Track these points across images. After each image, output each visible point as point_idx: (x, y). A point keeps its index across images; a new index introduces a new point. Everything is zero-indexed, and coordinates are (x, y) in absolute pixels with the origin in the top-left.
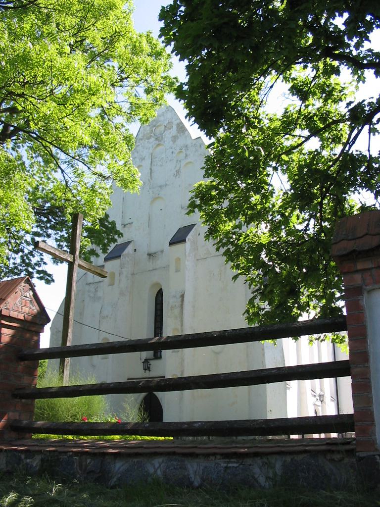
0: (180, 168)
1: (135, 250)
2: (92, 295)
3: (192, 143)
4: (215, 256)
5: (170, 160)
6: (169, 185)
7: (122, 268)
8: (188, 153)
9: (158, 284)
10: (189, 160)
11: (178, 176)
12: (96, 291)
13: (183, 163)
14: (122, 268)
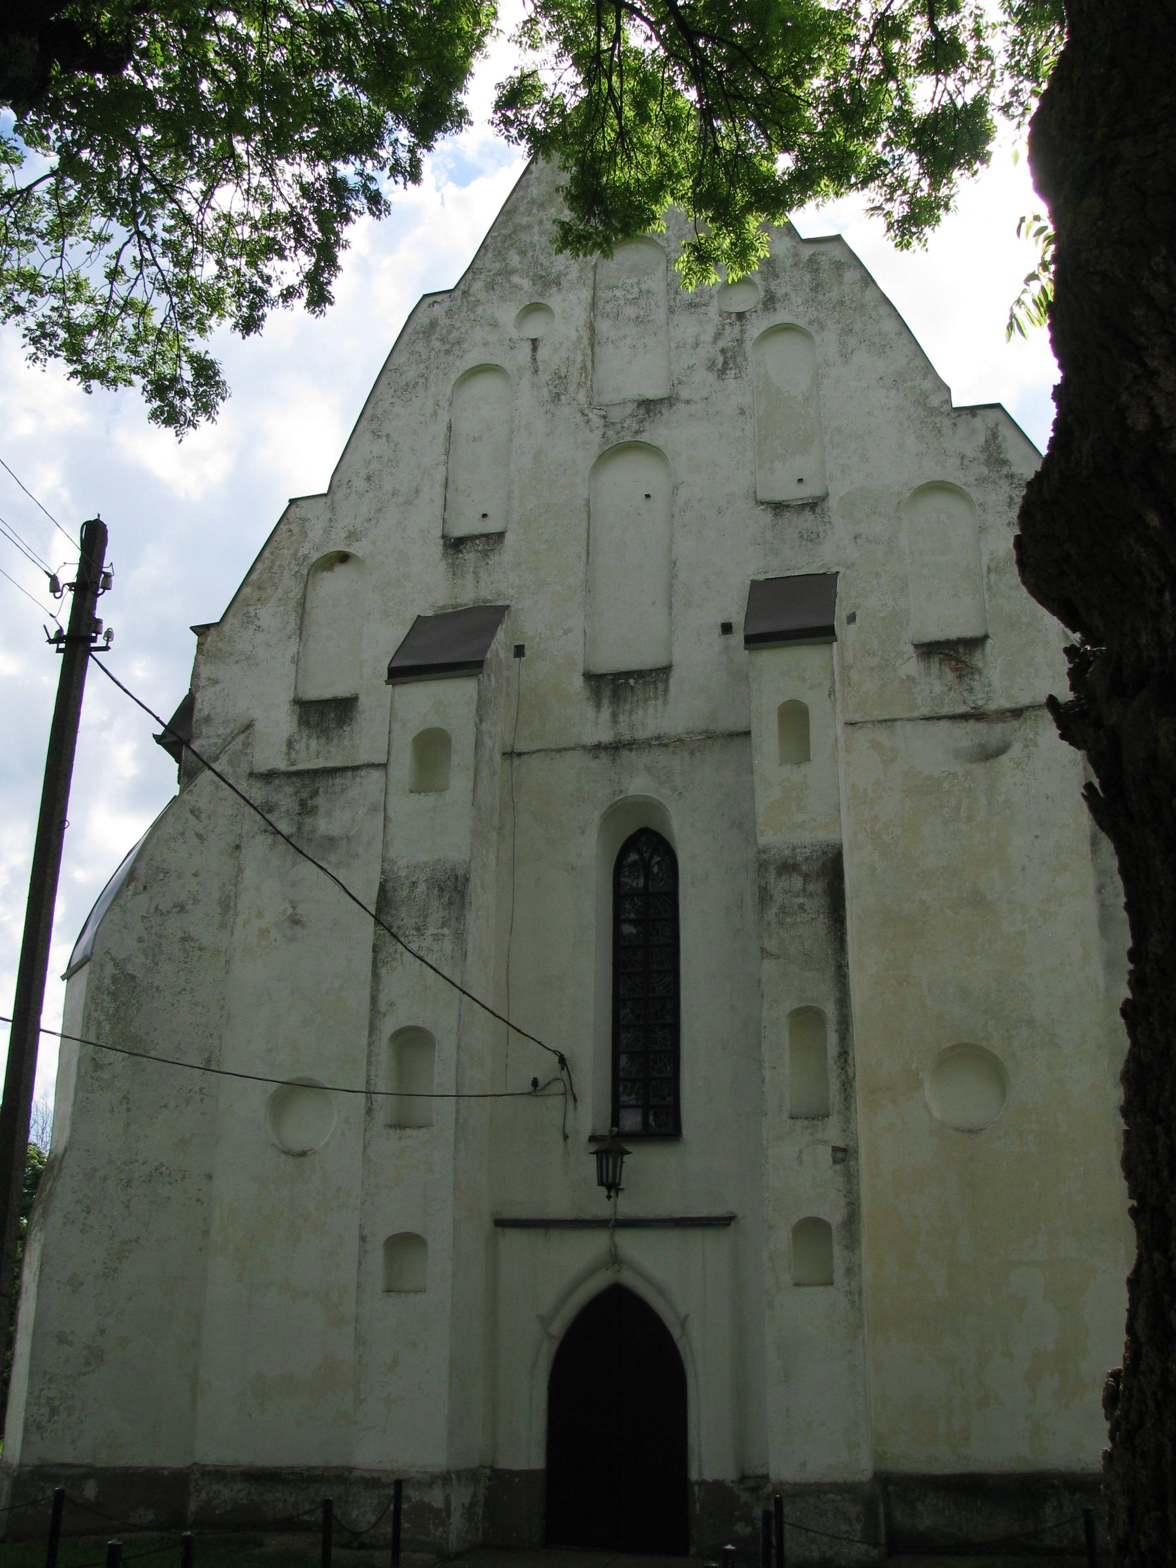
0: (740, 342)
1: (519, 651)
2: (284, 827)
3: (796, 255)
4: (953, 718)
5: (692, 306)
6: (688, 402)
7: (481, 721)
8: (780, 288)
9: (646, 805)
10: (782, 316)
11: (731, 374)
12: (306, 809)
13: (756, 327)
14: (481, 721)
